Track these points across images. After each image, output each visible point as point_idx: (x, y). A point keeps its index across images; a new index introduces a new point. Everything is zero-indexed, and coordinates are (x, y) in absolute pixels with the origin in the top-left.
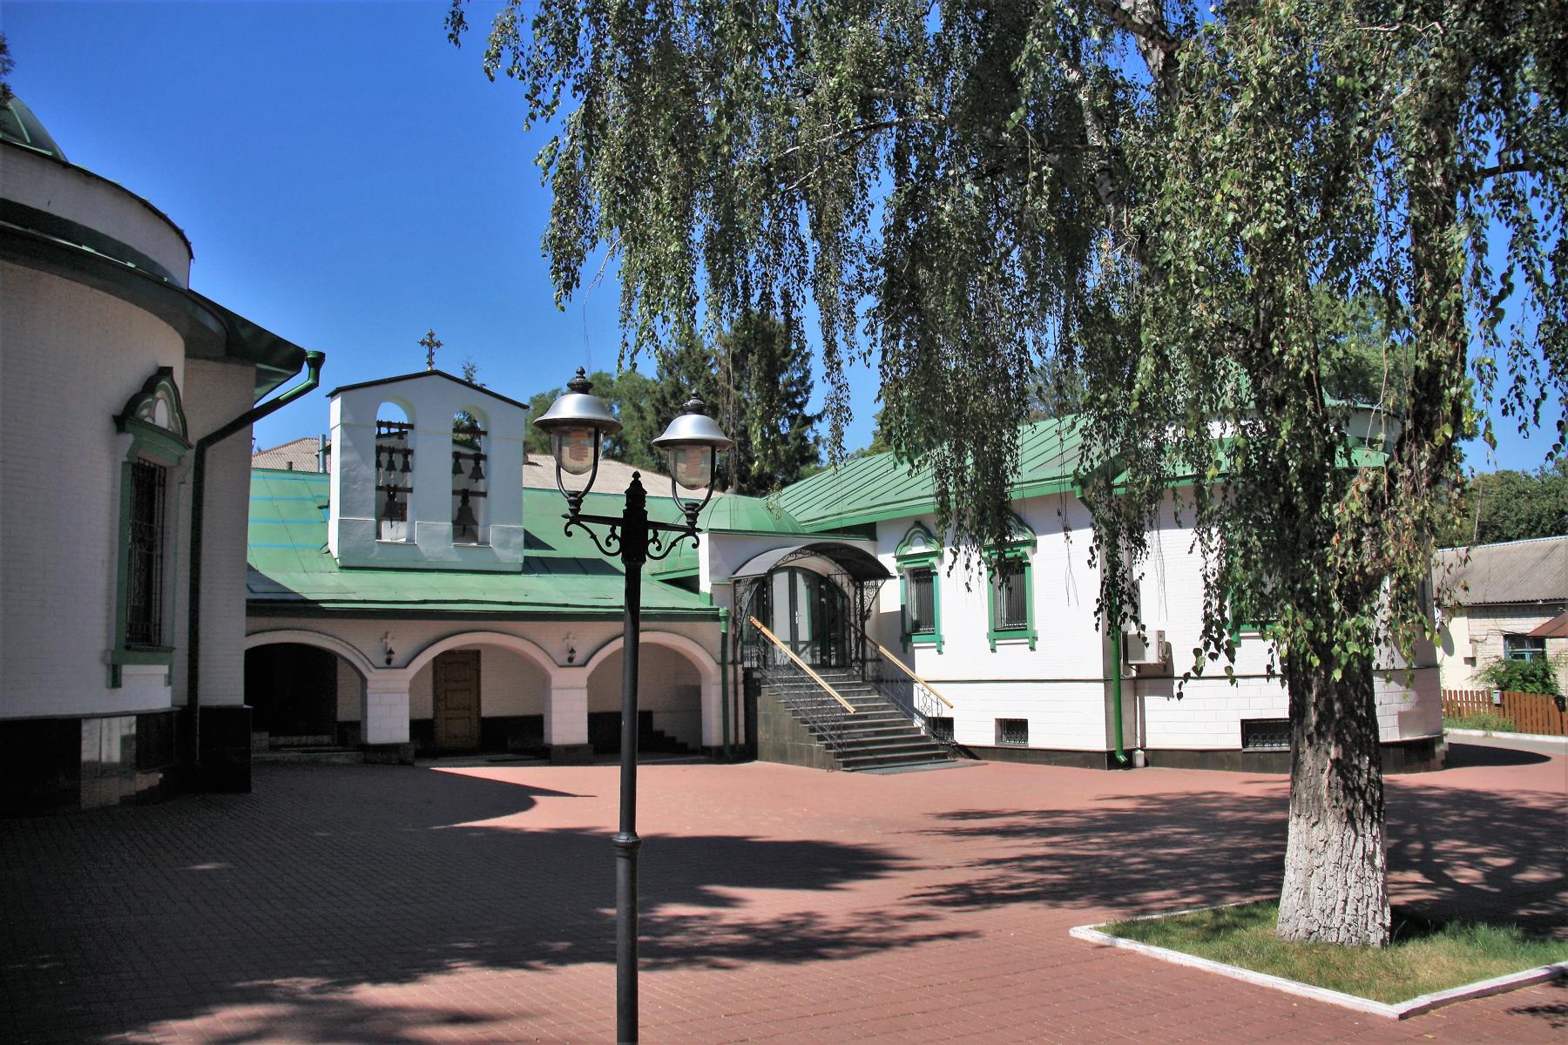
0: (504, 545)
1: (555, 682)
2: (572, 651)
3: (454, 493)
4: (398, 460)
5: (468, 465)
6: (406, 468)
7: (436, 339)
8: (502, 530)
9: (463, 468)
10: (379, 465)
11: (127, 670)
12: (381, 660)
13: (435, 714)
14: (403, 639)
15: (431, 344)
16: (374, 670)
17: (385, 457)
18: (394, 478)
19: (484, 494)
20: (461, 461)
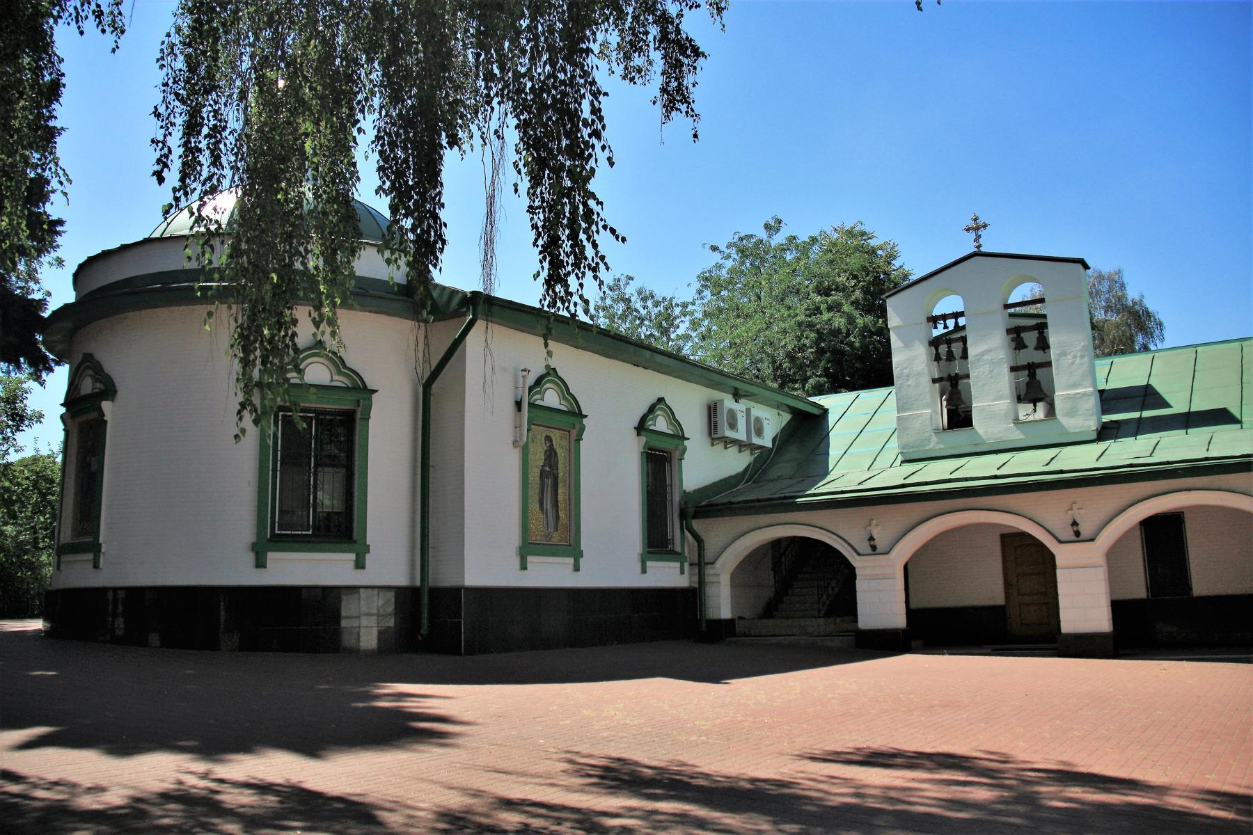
0: (1071, 413)
1: (1059, 562)
2: (1075, 524)
3: (1013, 369)
4: (957, 348)
5: (1030, 338)
6: (965, 355)
7: (980, 222)
8: (1069, 397)
9: (1027, 342)
10: (937, 358)
11: (271, 556)
12: (864, 547)
13: (1006, 602)
14: (884, 524)
15: (977, 227)
16: (857, 557)
17: (943, 349)
18: (957, 368)
19: (1049, 364)
20: (1022, 335)
